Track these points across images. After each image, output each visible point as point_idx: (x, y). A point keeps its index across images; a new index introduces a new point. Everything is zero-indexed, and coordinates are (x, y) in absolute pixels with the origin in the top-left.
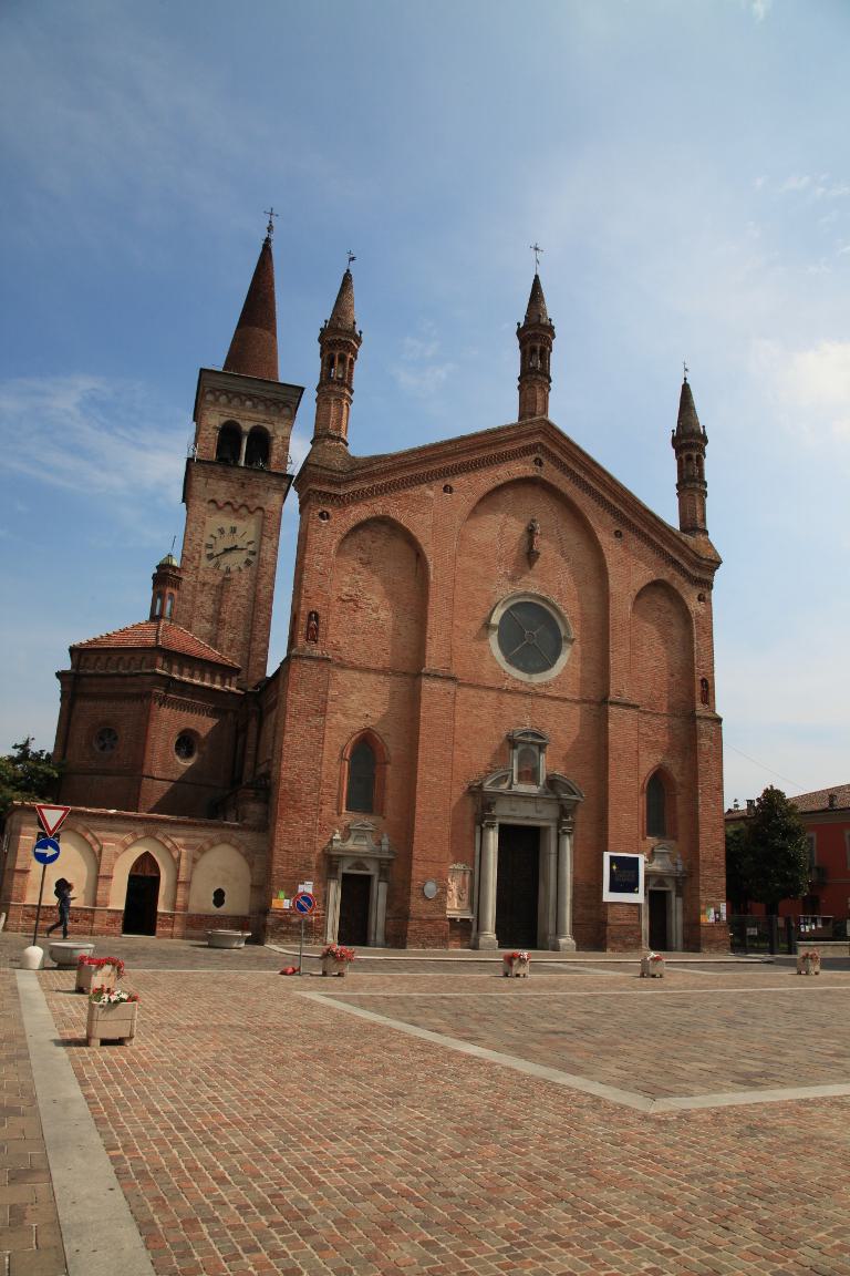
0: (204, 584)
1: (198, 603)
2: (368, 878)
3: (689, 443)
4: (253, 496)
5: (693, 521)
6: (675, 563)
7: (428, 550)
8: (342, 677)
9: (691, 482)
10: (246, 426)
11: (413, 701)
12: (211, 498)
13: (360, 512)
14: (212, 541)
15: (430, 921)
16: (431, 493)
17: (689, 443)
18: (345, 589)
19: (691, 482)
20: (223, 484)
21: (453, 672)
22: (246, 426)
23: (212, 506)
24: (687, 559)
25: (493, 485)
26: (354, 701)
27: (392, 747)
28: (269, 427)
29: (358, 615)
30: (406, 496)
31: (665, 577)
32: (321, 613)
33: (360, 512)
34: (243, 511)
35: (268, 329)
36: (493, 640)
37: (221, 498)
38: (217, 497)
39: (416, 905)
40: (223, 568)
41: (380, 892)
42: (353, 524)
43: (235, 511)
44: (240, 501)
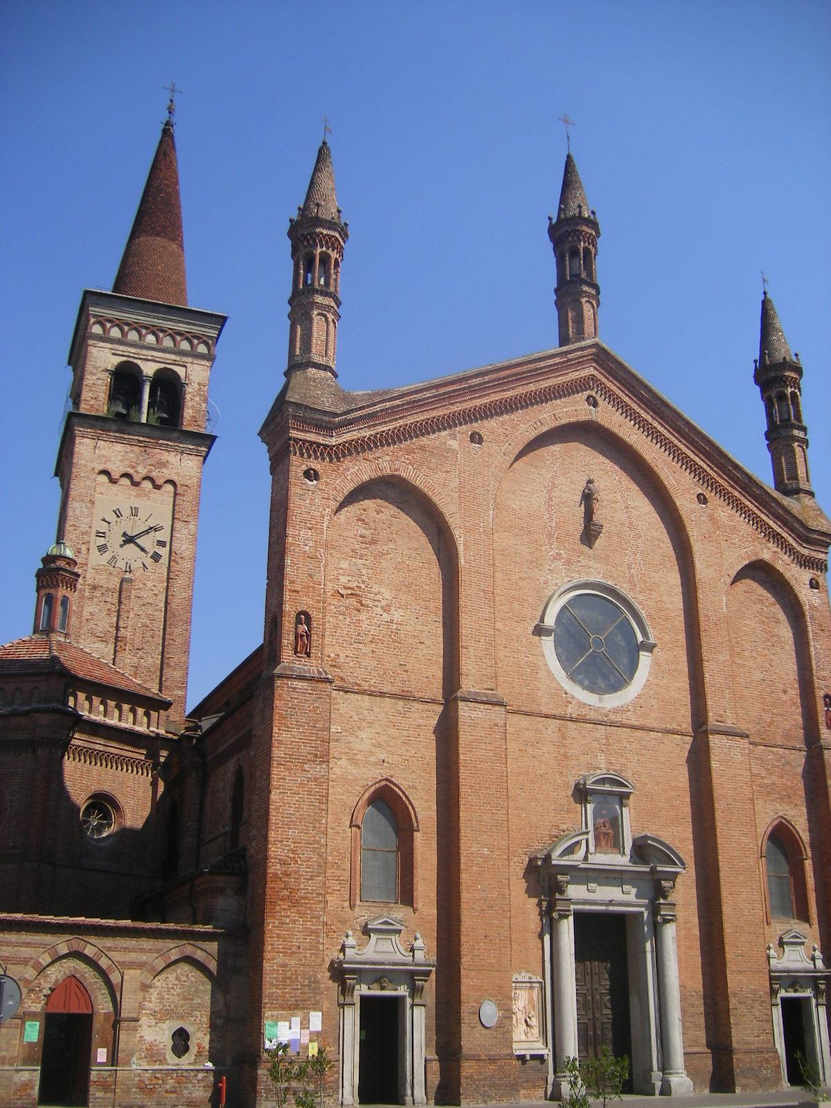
0: (95, 588)
1: (86, 615)
2: (396, 1002)
3: (775, 379)
4: (163, 464)
5: (788, 483)
6: (776, 537)
7: (455, 522)
8: (346, 705)
9: (783, 431)
10: (149, 369)
11: (447, 733)
12: (101, 467)
13: (359, 470)
14: (104, 527)
15: (492, 1060)
16: (454, 444)
17: (775, 379)
18: (344, 580)
19: (783, 431)
20: (119, 447)
21: (501, 693)
22: (149, 369)
23: (104, 478)
24: (792, 529)
25: (534, 434)
26: (363, 740)
27: (424, 808)
28: (180, 371)
29: (363, 616)
30: (422, 448)
31: (766, 556)
32: (314, 614)
33: (359, 470)
34: (147, 485)
35: (173, 240)
36: (548, 643)
37: (116, 469)
38: (109, 467)
39: (471, 1039)
40: (121, 564)
41: (418, 1026)
42: (350, 487)
43: (135, 484)
44: (142, 471)
